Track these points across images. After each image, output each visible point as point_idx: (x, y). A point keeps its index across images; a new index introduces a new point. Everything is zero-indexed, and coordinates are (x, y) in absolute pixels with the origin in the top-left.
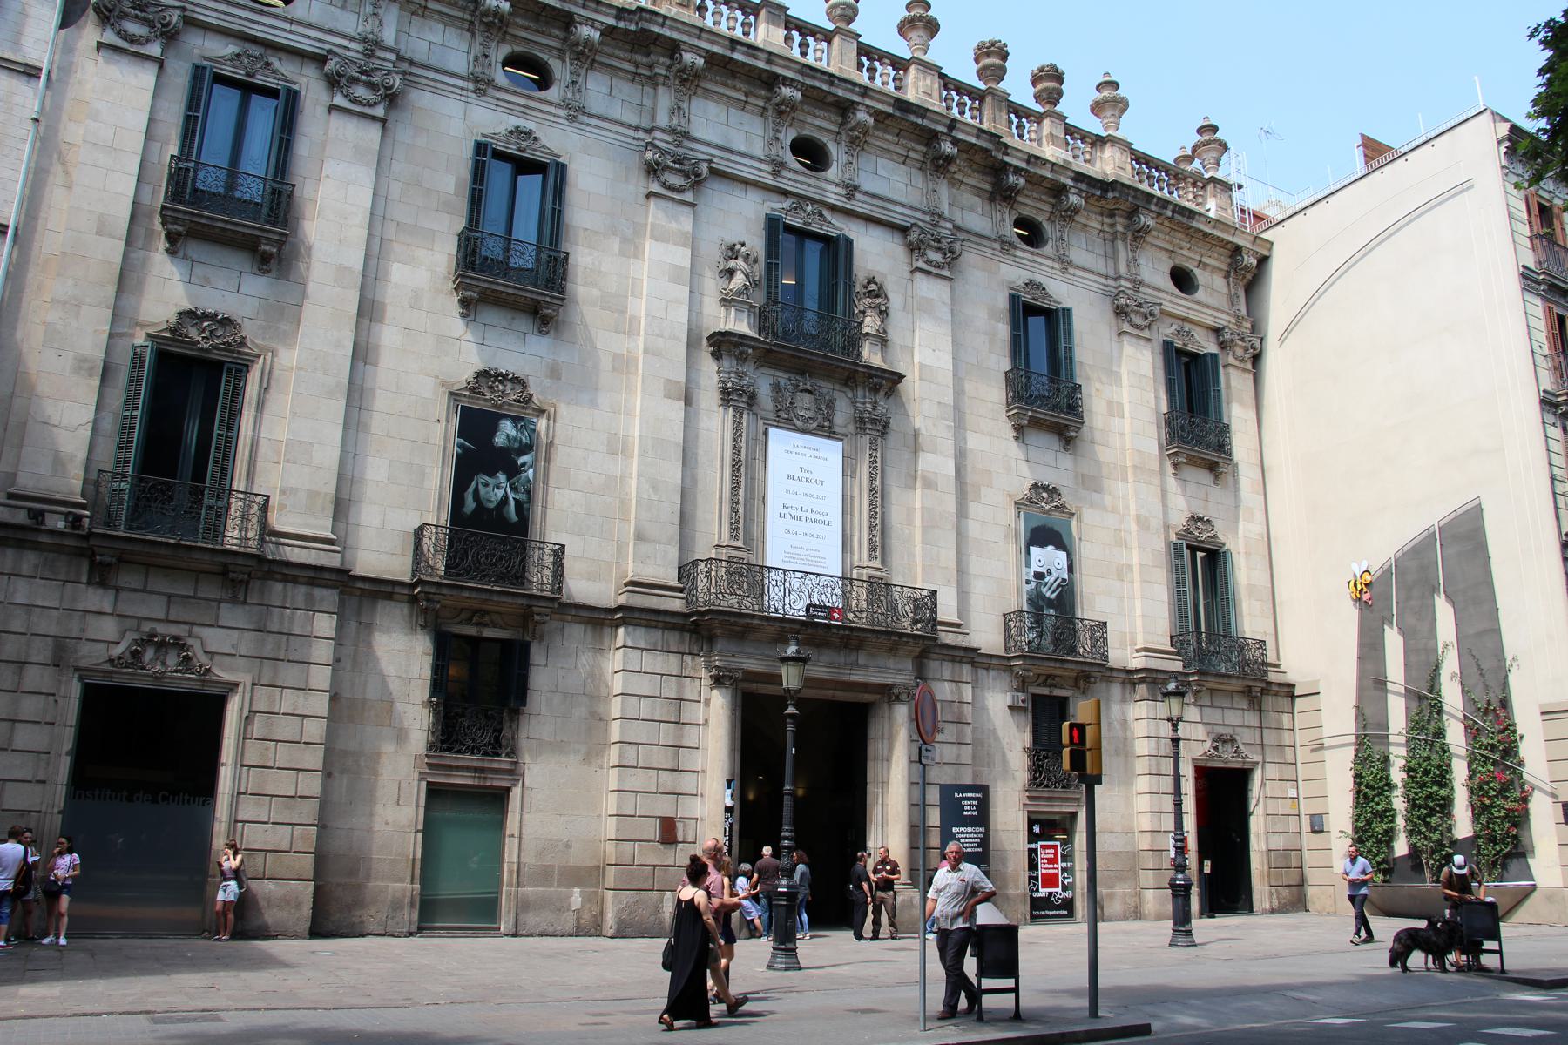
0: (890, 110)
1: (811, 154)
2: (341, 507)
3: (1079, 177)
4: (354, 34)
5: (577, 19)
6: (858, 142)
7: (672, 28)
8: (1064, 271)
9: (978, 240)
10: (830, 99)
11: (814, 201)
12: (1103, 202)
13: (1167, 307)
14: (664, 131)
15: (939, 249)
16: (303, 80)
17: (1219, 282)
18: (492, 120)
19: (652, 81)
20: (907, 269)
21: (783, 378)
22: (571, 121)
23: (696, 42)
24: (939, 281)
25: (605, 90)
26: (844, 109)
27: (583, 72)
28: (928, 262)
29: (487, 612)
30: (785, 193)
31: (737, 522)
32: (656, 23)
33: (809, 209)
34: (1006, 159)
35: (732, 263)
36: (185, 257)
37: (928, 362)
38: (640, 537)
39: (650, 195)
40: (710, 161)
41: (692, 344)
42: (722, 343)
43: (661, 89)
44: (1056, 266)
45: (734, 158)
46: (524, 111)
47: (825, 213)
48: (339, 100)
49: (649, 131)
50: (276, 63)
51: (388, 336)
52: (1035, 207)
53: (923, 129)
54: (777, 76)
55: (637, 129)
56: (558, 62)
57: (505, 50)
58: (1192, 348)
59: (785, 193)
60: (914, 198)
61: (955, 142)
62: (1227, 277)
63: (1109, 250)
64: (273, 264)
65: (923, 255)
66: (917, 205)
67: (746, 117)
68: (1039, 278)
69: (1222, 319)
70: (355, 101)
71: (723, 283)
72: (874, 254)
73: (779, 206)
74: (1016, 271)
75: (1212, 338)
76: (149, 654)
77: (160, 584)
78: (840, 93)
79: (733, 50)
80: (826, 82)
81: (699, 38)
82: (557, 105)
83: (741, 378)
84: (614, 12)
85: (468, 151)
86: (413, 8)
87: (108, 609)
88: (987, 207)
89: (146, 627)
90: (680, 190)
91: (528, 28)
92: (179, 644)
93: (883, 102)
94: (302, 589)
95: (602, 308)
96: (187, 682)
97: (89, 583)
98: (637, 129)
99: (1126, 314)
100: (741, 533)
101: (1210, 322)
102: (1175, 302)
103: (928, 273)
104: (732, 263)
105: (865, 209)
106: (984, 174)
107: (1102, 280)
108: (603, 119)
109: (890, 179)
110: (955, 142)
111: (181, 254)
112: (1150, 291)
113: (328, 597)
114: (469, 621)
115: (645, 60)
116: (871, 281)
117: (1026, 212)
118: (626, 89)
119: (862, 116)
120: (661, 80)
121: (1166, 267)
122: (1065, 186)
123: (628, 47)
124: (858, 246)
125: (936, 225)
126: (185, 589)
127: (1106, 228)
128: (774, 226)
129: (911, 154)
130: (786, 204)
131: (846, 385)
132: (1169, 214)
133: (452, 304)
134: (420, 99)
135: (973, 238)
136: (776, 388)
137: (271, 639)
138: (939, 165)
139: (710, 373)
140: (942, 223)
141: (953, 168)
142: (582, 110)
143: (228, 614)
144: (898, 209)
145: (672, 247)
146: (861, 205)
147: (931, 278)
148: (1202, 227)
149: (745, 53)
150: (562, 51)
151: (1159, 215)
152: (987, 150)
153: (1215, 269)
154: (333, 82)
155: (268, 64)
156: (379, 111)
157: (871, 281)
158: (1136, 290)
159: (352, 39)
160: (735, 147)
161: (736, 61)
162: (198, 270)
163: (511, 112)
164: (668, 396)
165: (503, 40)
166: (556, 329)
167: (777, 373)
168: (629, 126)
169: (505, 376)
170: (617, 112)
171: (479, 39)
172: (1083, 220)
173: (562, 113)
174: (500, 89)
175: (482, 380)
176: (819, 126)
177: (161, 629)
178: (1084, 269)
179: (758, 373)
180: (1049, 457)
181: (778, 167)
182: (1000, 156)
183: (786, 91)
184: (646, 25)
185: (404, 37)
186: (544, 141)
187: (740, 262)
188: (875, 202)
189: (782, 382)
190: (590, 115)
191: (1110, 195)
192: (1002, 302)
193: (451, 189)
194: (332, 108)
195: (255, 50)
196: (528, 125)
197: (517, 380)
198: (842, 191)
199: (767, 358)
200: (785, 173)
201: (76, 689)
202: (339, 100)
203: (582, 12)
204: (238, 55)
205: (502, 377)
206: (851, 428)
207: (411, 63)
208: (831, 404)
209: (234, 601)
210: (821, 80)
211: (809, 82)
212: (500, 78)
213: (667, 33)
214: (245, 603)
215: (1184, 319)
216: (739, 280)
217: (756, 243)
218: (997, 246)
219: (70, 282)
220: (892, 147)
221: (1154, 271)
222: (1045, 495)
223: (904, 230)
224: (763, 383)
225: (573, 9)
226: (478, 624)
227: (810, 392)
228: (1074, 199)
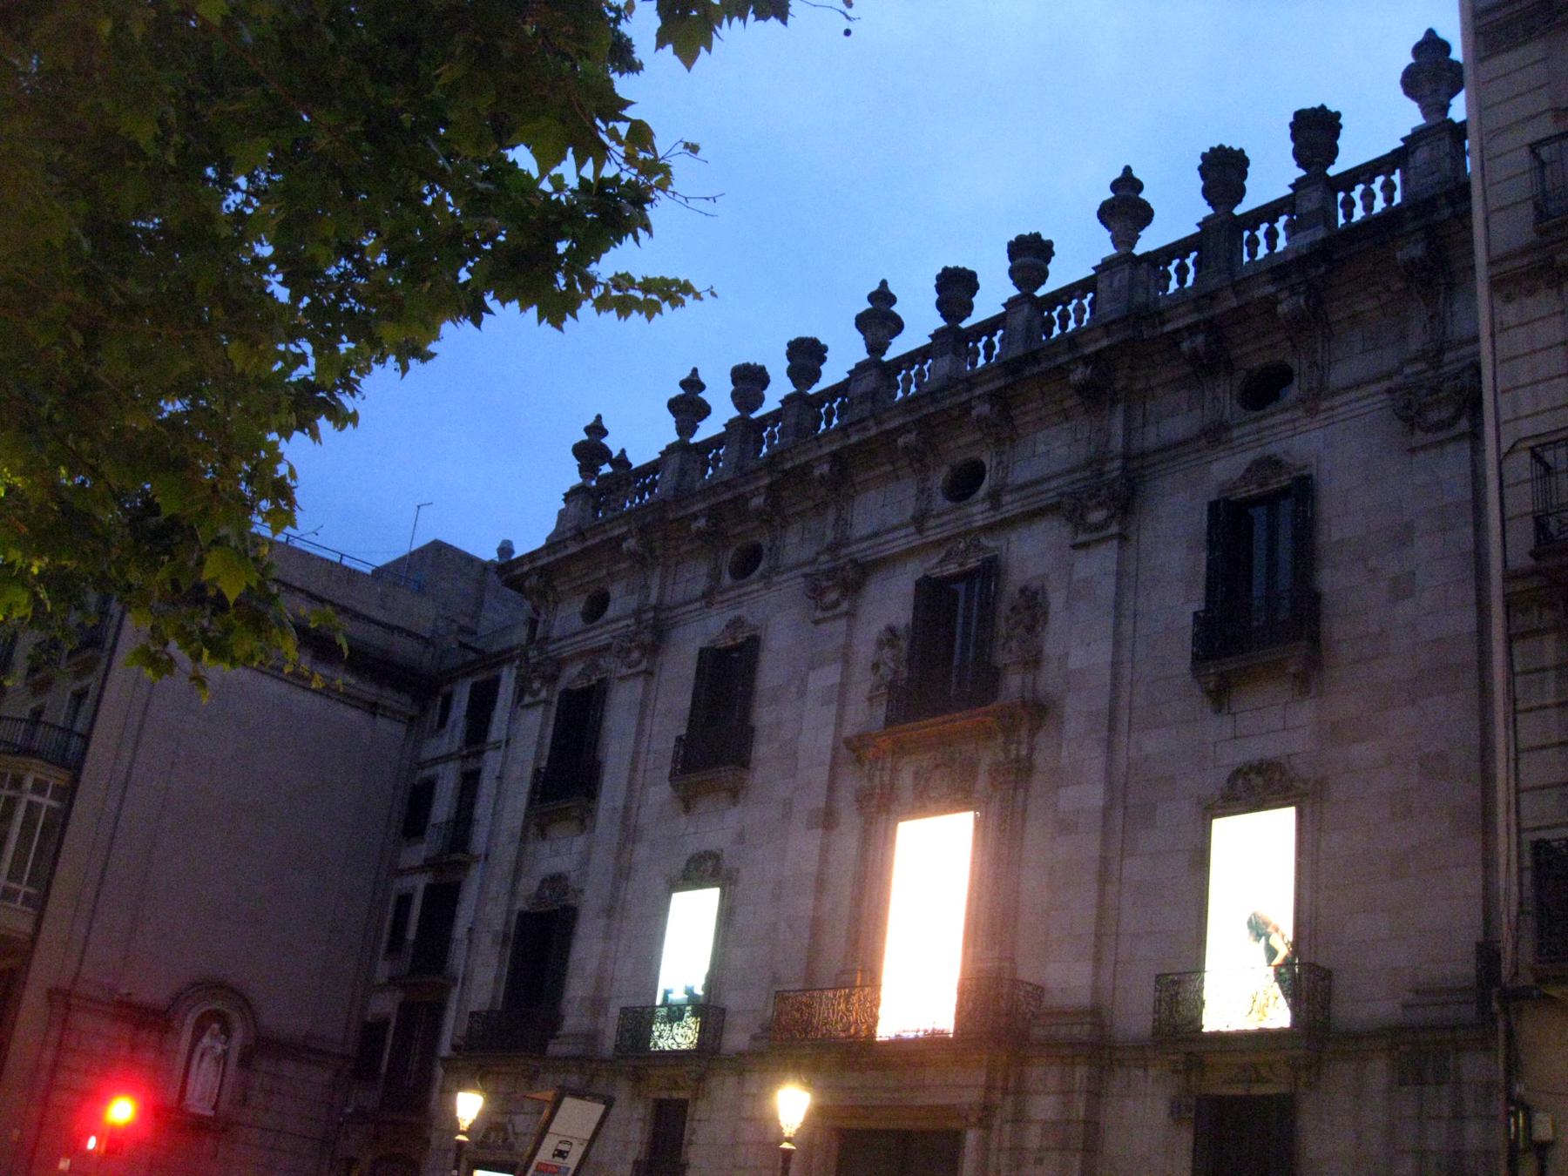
30: (939, 544)
61: (1086, 360)
68: (1274, 449)
93: (991, 380)
110: (1086, 360)
125: (1101, 473)
129: (1068, 404)
169: (701, 857)
188: (1023, 494)
189: (925, 764)
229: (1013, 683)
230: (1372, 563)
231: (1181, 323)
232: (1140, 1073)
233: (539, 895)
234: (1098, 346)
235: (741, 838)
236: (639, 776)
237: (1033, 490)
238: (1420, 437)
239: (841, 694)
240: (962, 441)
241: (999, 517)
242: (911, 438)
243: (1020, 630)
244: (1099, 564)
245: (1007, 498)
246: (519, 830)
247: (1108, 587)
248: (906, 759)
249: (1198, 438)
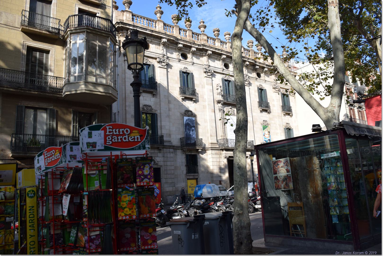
2: (170, 135)
3: (267, 65)
30: (223, 74)
38: (211, 136)
42: (219, 102)
59: (223, 74)
61: (249, 62)
68: (261, 84)
71: (217, 91)
85: (179, 72)
90: (210, 76)
94: (168, 149)
104: (218, 88)
110: (249, 62)
113: (171, 150)
117: (258, 72)
130: (224, 76)
142: (194, 63)
156: (166, 67)
162: (145, 98)
192: (256, 89)
193: (177, 79)
196: (186, 66)
209: (159, 152)
212: (181, 59)
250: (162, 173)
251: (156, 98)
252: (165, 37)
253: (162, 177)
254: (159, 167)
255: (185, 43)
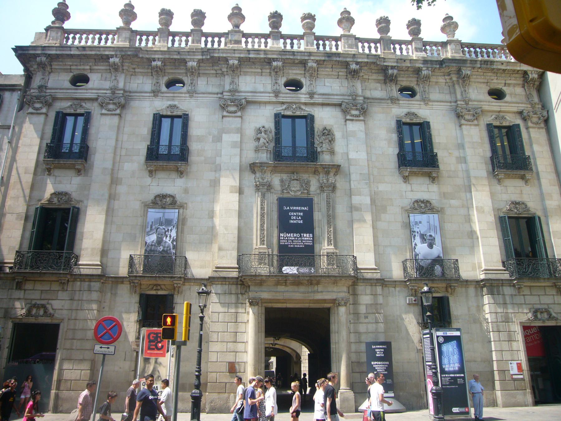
0: (323, 58)
1: (295, 85)
3: (425, 61)
4: (108, 87)
5: (187, 60)
6: (314, 75)
7: (222, 53)
8: (426, 104)
9: (379, 101)
10: (297, 61)
11: (295, 103)
12: (443, 70)
13: (486, 108)
14: (227, 92)
15: (357, 109)
16: (93, 108)
17: (519, 90)
18: (160, 105)
19: (223, 74)
20: (343, 120)
21: (285, 176)
22: (191, 97)
23: (233, 55)
24: (358, 122)
25: (205, 83)
26: (303, 63)
27: (195, 78)
28: (353, 116)
29: (159, 285)
30: (283, 103)
31: (264, 237)
32: (216, 53)
33: (294, 106)
34: (385, 64)
35: (259, 136)
36: (54, 176)
37: (354, 157)
39: (223, 117)
40: (245, 98)
41: (241, 170)
42: (253, 167)
43: (226, 77)
44: (422, 103)
45: (258, 94)
46: (173, 98)
47: (303, 107)
48: (104, 111)
49: (222, 93)
50: (84, 104)
51: (121, 189)
52: (405, 82)
53: (341, 62)
54: (270, 59)
55: (217, 94)
56: (186, 78)
57: (166, 79)
58: (505, 124)
60: (344, 90)
61: (357, 63)
62: (523, 87)
63: (452, 90)
64: (82, 172)
65: (348, 113)
66: (345, 94)
67: (263, 77)
68: (413, 110)
69: (521, 107)
70: (109, 111)
71: (256, 144)
72: (325, 117)
73: (281, 108)
74: (403, 108)
75: (518, 117)
76: (34, 311)
77: (39, 286)
78: (299, 58)
79: (249, 54)
80: (292, 55)
81: (234, 53)
82: (185, 93)
83: (263, 179)
84: (200, 53)
86: (131, 73)
87: (22, 297)
88: (384, 86)
89: (33, 302)
90: (235, 112)
91: (172, 69)
92: (44, 306)
94: (87, 283)
95: (205, 164)
96: (47, 320)
97: (16, 289)
98: (217, 94)
99: (462, 116)
100: (265, 242)
101: (515, 109)
102: (494, 105)
103: (352, 120)
104: (259, 136)
105: (320, 101)
106: (378, 73)
107: (449, 104)
108: (204, 93)
109: (332, 86)
110: (357, 63)
111: (52, 175)
112: (476, 103)
114: (152, 289)
115: (218, 68)
116: (325, 129)
118: (214, 81)
119: (310, 64)
120: (225, 73)
121: (486, 89)
122: (419, 68)
123: (211, 65)
124: (316, 116)
125: (355, 100)
126: (46, 287)
127: (448, 81)
128: (278, 118)
129: (340, 74)
130: (284, 107)
131: (315, 174)
132: (479, 66)
133: (146, 174)
134: (135, 104)
135: (376, 101)
136: (282, 181)
137: (75, 302)
138: (354, 74)
139: (250, 180)
140: (358, 98)
141: (361, 74)
143: (61, 295)
144: (336, 97)
145: (232, 135)
146: (318, 99)
147: (354, 122)
148: (499, 67)
149: (254, 54)
150: (186, 73)
151: (474, 68)
152: (374, 63)
153: (515, 85)
154: (101, 106)
155: (81, 106)
156: (118, 111)
157: (325, 129)
158: (467, 104)
159: (107, 90)
160: (258, 91)
161: (252, 58)
162: (58, 179)
163: (168, 100)
164: (231, 192)
165: (165, 75)
166: (187, 175)
167: (282, 175)
168: (214, 94)
170: (210, 89)
171: (155, 77)
172: (434, 80)
173: (187, 95)
174: (163, 93)
175: (158, 199)
176: (295, 73)
177: (39, 302)
178: (437, 101)
179: (273, 176)
180: (424, 188)
181: (277, 93)
182: (382, 64)
183: (275, 64)
184: (212, 55)
185: (128, 85)
186: (181, 107)
187: (263, 134)
189: (285, 178)
190: (198, 94)
191: (444, 66)
192: (393, 124)
194: (102, 114)
195: (76, 102)
196: (176, 103)
197: (170, 196)
198: (308, 96)
199: (275, 170)
200: (281, 95)
201: (10, 325)
202: (104, 111)
203: (189, 57)
204: (71, 105)
205: (164, 196)
206: (318, 191)
207: (130, 92)
208: (308, 183)
209: (63, 290)
210: (290, 55)
211: (284, 57)
213: (221, 55)
214: (67, 290)
215: (499, 112)
216: (262, 140)
217: (270, 125)
218: (389, 101)
219: (16, 191)
220: (330, 73)
221: (477, 93)
222: (423, 205)
223: (340, 105)
224: (276, 180)
225: (185, 57)
226: (155, 290)
227: (297, 180)
228: (425, 72)
229: (325, 159)
230: (450, 151)
231: (390, 64)
232: (393, 289)
233: (50, 201)
234: (363, 60)
235: (186, 191)
236: (118, 158)
237: (327, 97)
238: (463, 122)
239: (241, 145)
240: (294, 72)
241: (312, 102)
242: (280, 64)
243: (328, 141)
244: (355, 127)
245: (316, 96)
246: (32, 169)
247: (362, 135)
248: (276, 175)
249: (388, 99)
250: (60, 337)
251: (86, 174)
252: (113, 53)
253: (58, 346)
254: (55, 322)
255: (167, 56)
